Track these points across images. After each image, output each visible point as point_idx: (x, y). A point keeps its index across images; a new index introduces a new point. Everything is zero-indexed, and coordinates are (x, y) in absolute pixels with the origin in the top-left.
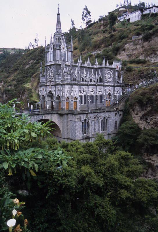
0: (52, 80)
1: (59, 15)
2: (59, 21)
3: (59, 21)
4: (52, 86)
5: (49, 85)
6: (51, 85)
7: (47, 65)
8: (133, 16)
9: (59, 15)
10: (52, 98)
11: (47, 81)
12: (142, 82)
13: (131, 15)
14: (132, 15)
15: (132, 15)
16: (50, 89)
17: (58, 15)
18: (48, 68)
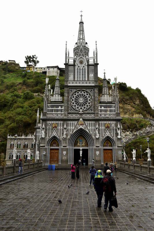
0: (86, 111)
1: (81, 23)
2: (81, 31)
3: (81, 31)
4: (86, 122)
5: (78, 120)
6: (84, 120)
7: (69, 85)
8: (50, 70)
9: (81, 23)
10: (75, 145)
11: (68, 111)
12: (125, 132)
13: (48, 69)
14: (49, 69)
15: (49, 69)
16: (81, 127)
17: (80, 23)
18: (75, 90)
